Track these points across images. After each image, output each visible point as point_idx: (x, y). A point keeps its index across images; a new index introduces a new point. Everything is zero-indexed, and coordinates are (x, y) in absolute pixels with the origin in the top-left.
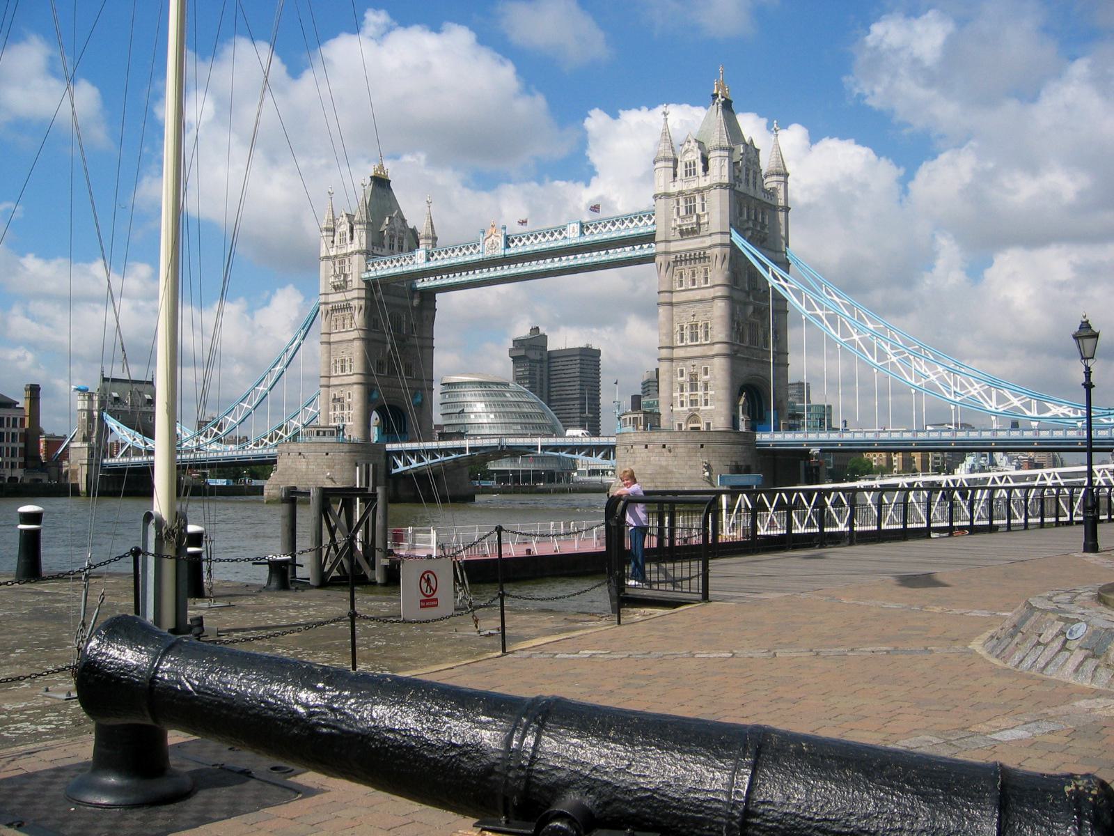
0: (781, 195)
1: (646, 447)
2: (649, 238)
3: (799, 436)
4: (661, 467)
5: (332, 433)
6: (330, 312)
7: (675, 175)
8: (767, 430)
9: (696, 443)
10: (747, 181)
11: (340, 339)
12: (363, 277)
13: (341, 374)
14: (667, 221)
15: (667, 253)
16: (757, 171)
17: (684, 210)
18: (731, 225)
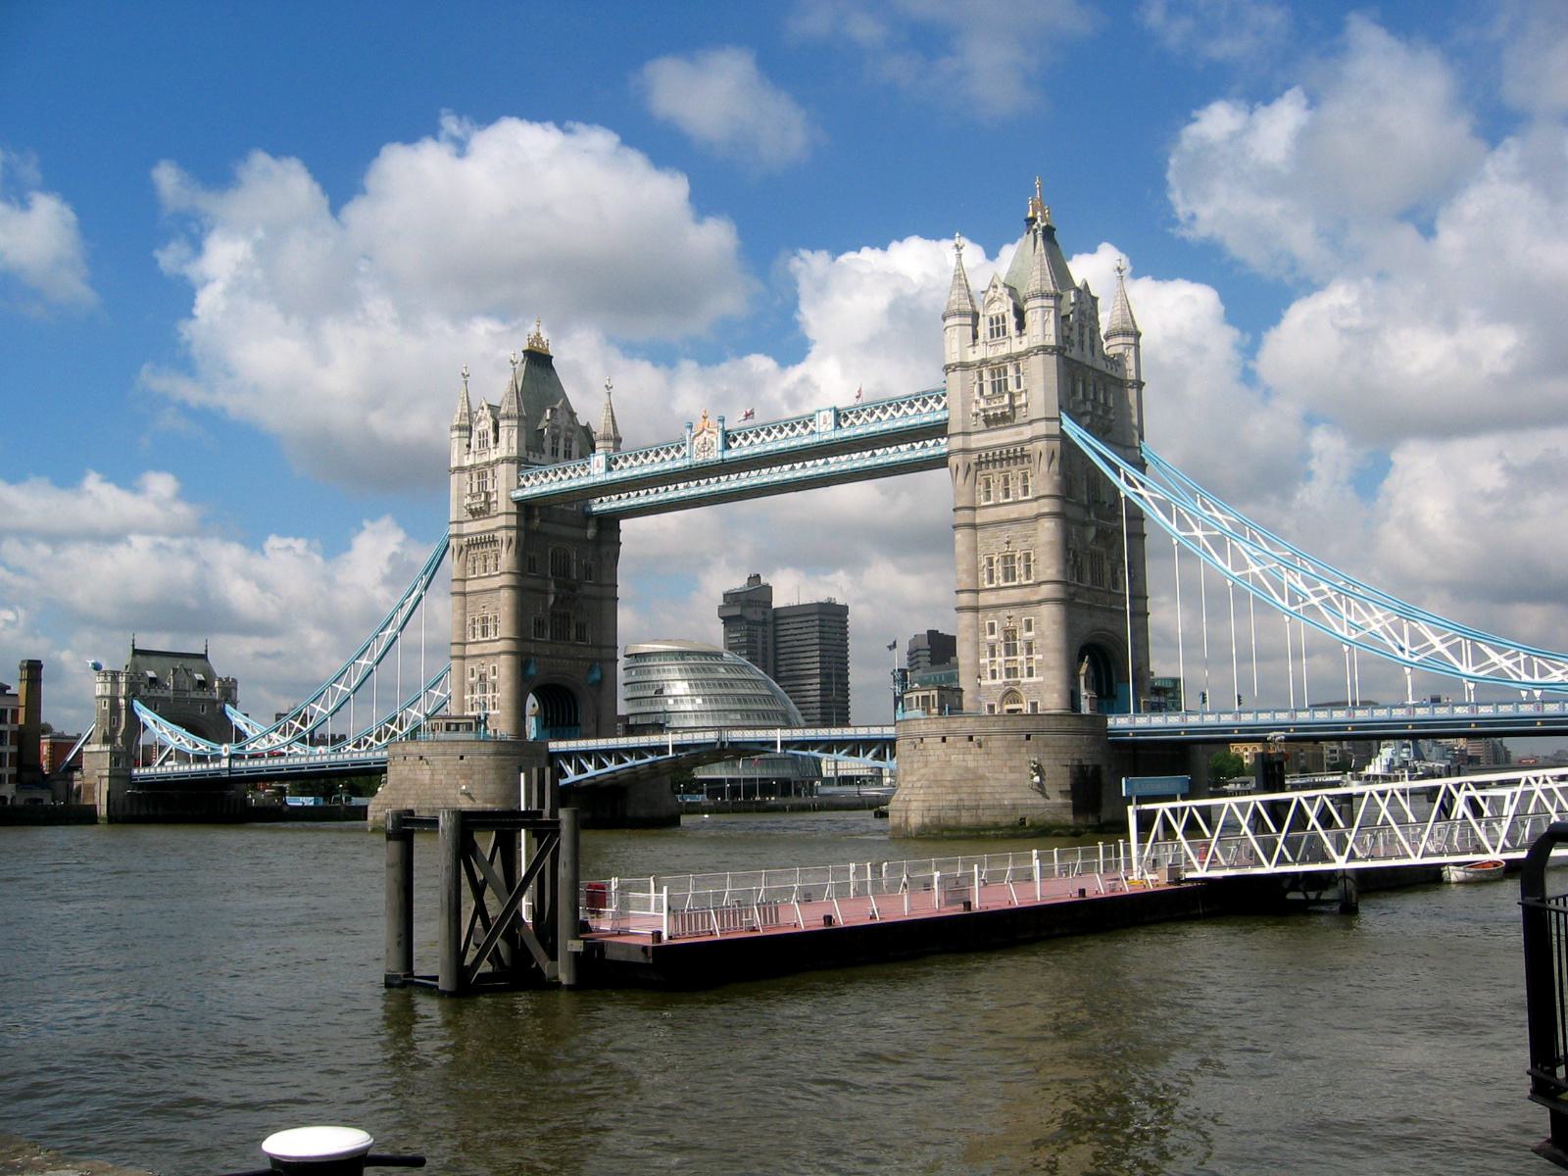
0: (1130, 364)
1: (944, 740)
2: (938, 430)
3: (1173, 720)
4: (967, 769)
5: (469, 727)
6: (465, 549)
7: (975, 336)
8: (1125, 711)
9: (1018, 733)
10: (1082, 343)
11: (480, 588)
12: (513, 496)
15: (965, 451)
16: (1095, 330)
17: (990, 388)
18: (1061, 407)
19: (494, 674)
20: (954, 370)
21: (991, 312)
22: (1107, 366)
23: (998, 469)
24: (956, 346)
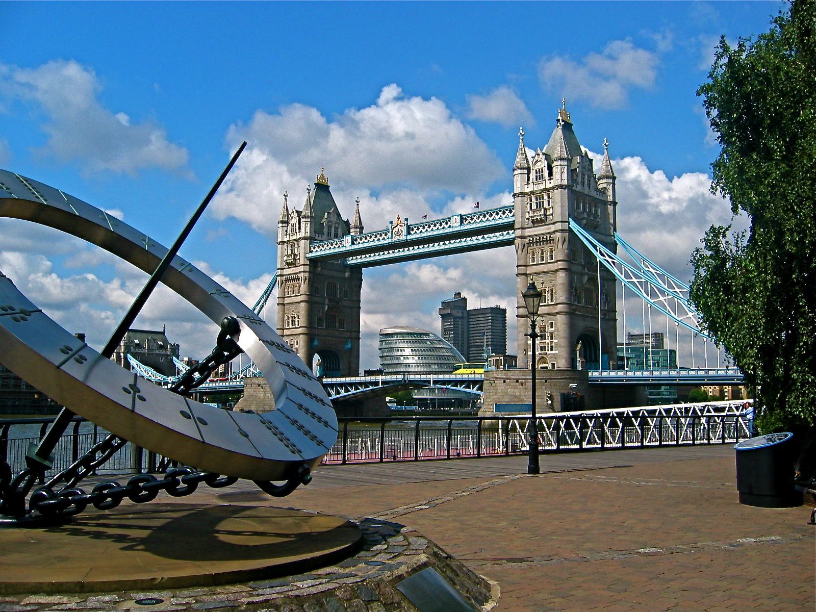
0: (610, 193)
2: (510, 226)
4: (515, 396)
6: (284, 282)
7: (528, 179)
8: (597, 369)
12: (307, 255)
13: (291, 327)
14: (523, 214)
15: (522, 237)
16: (592, 175)
18: (569, 216)
19: (297, 345)
20: (518, 197)
21: (536, 167)
22: (597, 194)
23: (539, 246)
24: (519, 185)
